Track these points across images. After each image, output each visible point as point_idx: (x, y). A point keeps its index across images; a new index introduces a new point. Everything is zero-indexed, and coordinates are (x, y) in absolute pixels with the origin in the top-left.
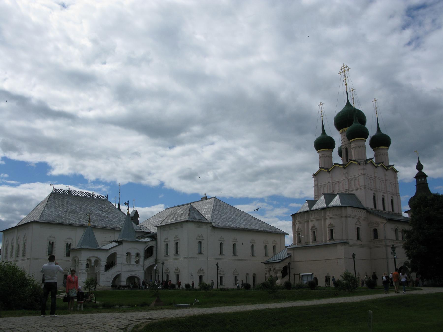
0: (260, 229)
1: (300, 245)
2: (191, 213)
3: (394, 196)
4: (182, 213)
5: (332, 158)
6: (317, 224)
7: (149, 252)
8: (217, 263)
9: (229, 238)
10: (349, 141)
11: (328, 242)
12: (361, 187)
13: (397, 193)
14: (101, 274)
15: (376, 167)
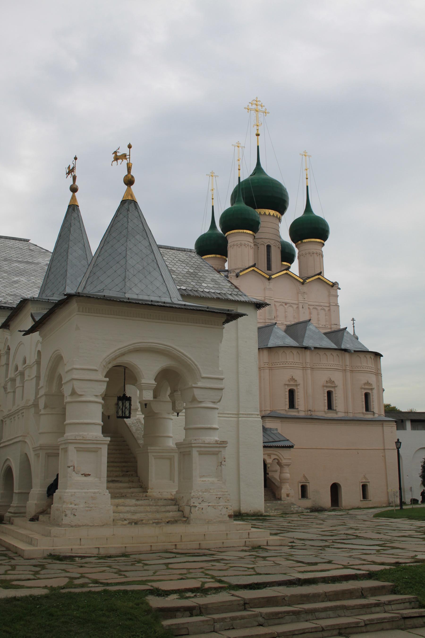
11: (360, 416)
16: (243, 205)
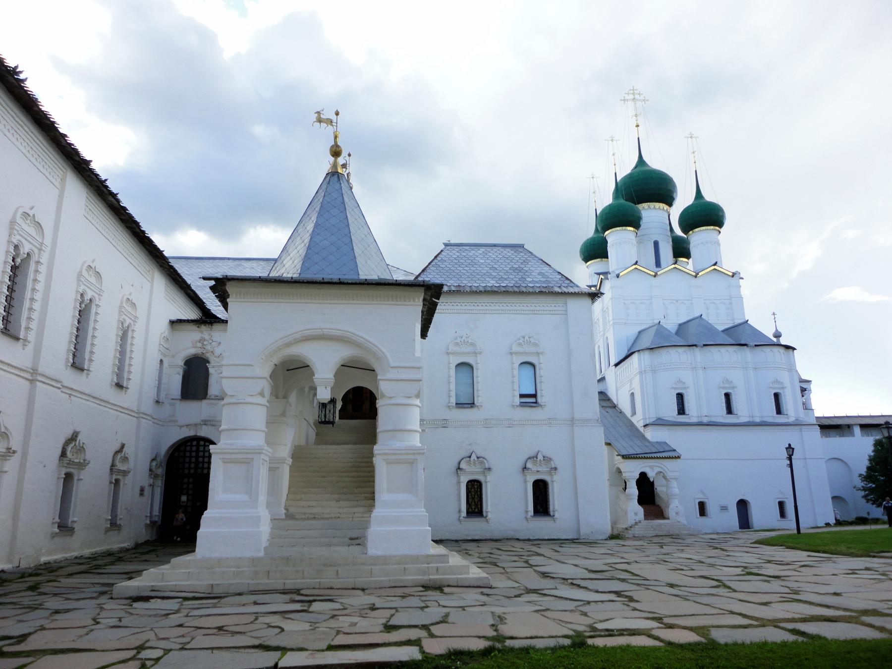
8: (790, 445)
11: (770, 420)
16: (622, 201)
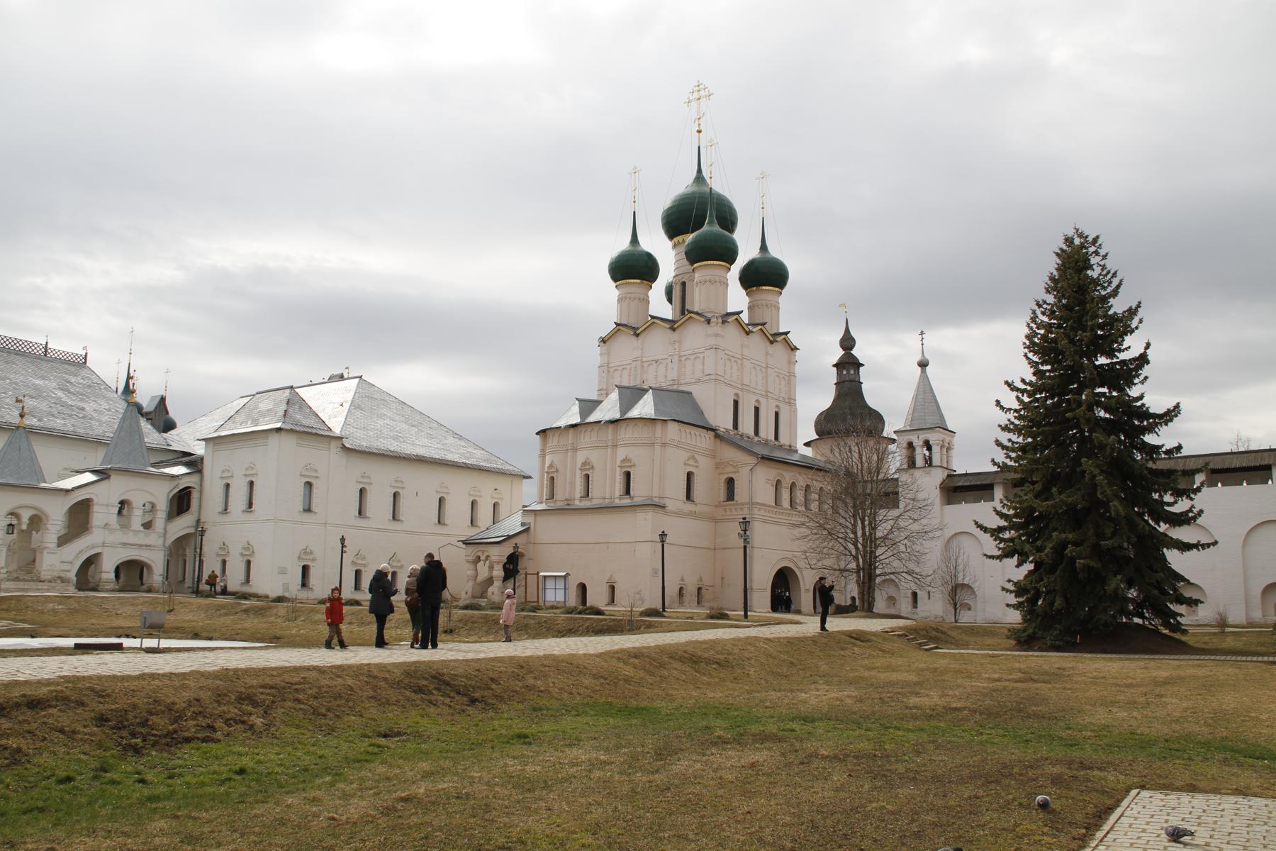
0: (464, 461)
1: (552, 505)
2: (291, 411)
3: (781, 405)
4: (269, 410)
5: (649, 303)
6: (595, 457)
7: (181, 502)
9: (382, 480)
10: (689, 266)
12: (708, 377)
13: (790, 399)
14: (45, 552)
15: (748, 333)
